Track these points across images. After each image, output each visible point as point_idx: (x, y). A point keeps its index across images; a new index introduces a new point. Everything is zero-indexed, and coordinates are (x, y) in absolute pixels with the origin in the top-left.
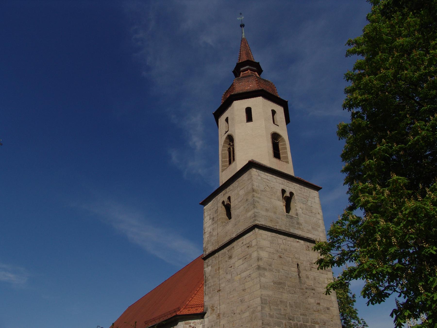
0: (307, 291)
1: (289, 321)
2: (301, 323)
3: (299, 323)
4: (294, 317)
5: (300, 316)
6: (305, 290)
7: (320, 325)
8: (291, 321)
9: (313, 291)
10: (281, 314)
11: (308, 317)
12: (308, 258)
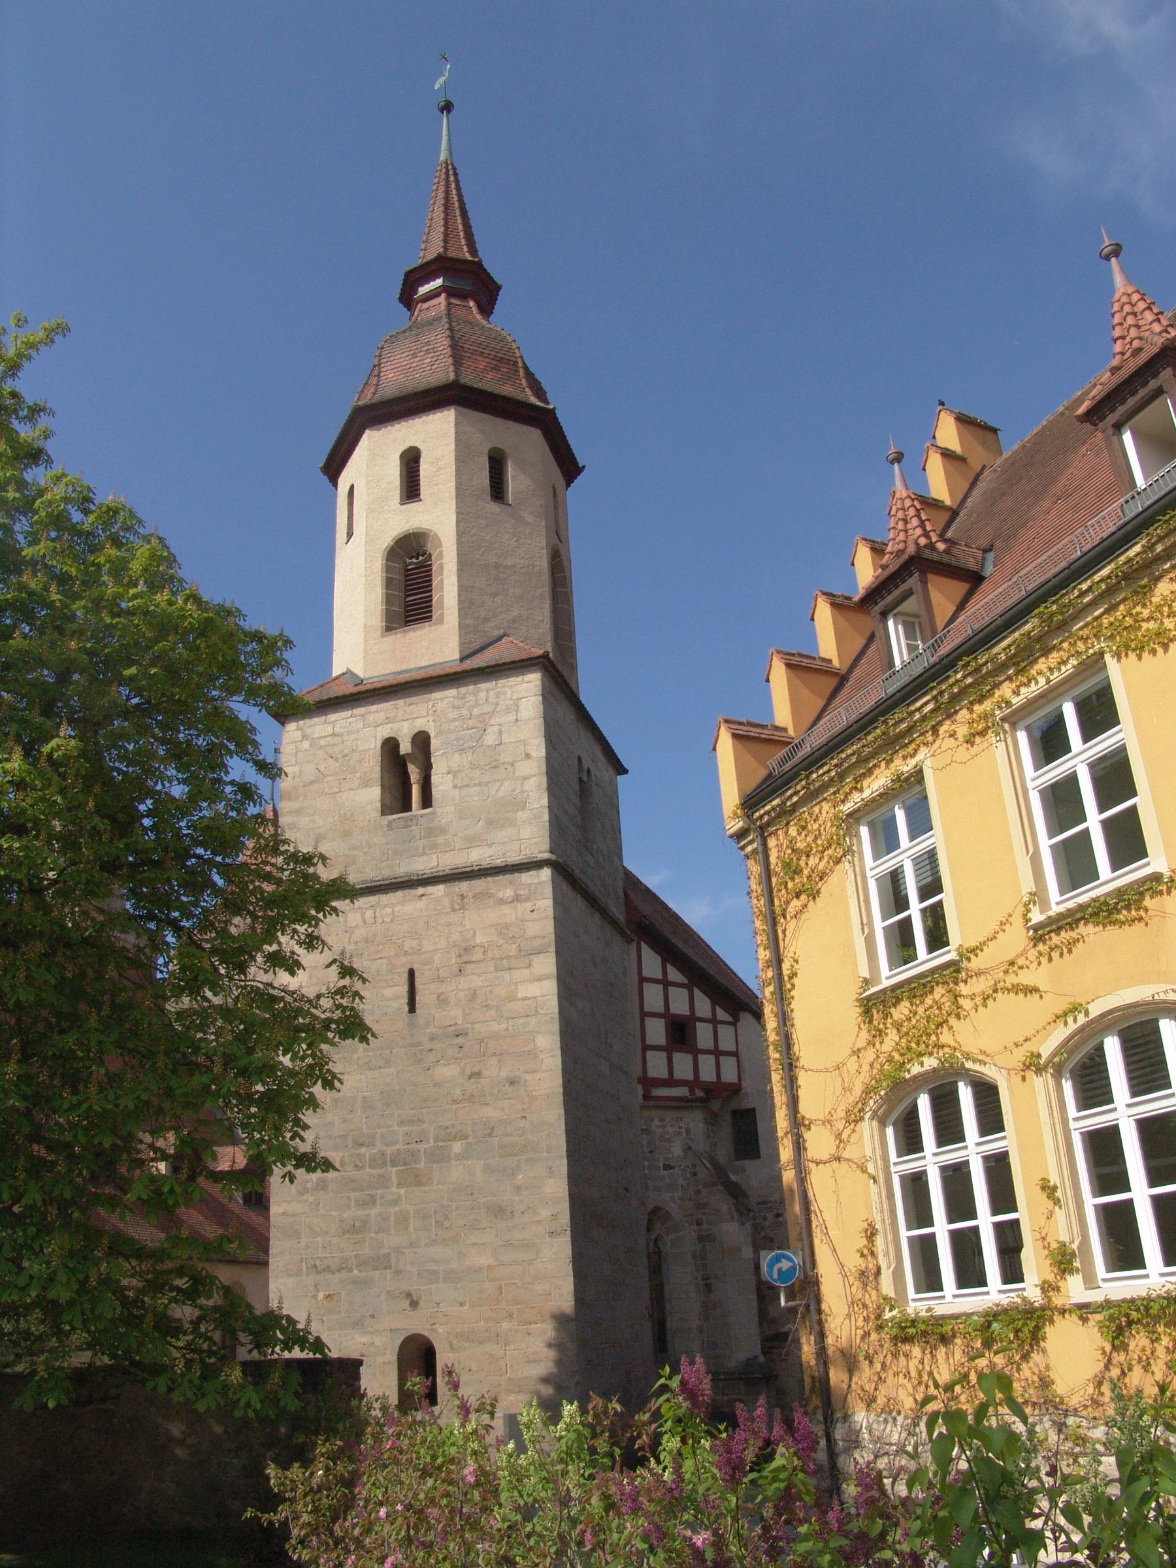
0: (437, 1045)
1: (357, 1151)
2: (397, 1147)
3: (389, 1151)
4: (373, 1137)
5: (396, 1128)
6: (428, 1046)
7: (470, 1140)
8: (363, 1150)
9: (460, 1040)
10: (331, 1138)
11: (425, 1125)
12: (455, 937)
